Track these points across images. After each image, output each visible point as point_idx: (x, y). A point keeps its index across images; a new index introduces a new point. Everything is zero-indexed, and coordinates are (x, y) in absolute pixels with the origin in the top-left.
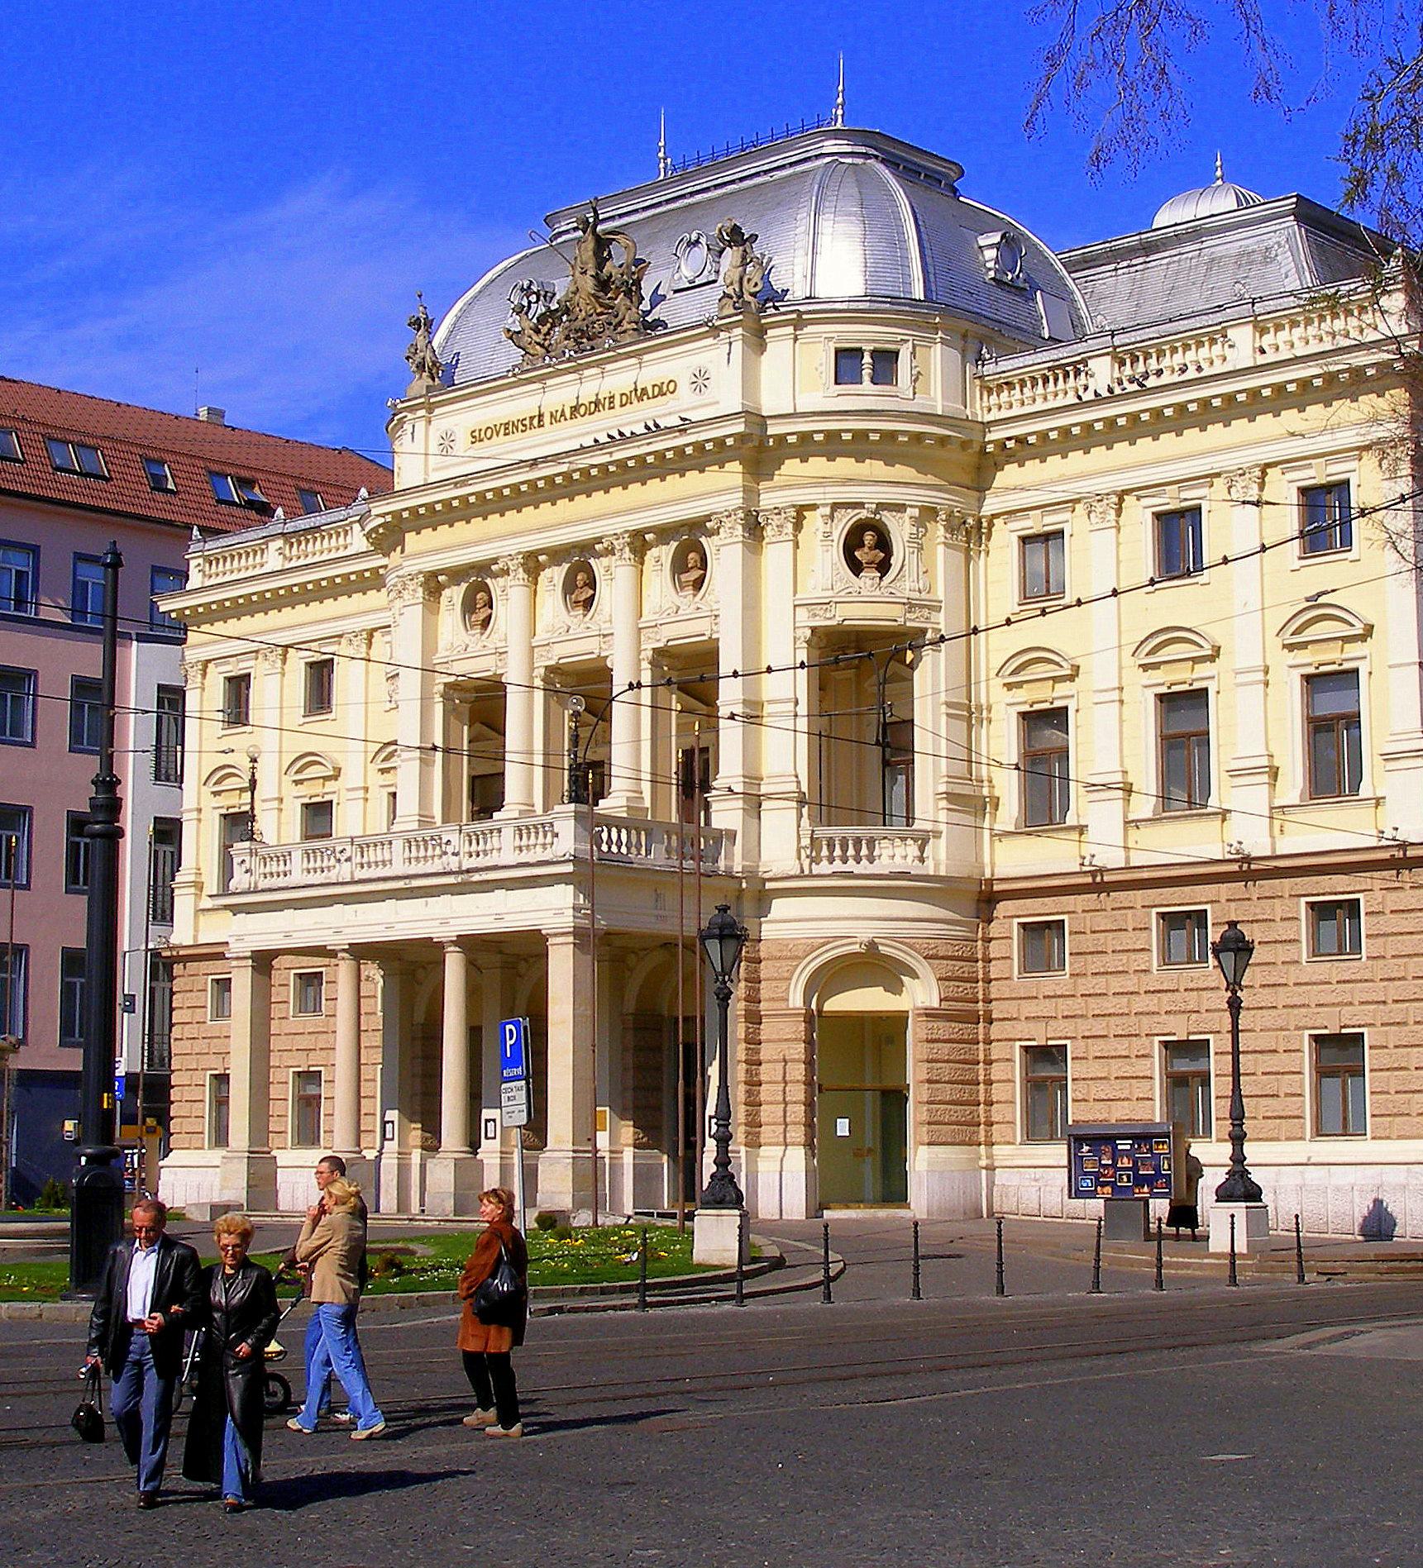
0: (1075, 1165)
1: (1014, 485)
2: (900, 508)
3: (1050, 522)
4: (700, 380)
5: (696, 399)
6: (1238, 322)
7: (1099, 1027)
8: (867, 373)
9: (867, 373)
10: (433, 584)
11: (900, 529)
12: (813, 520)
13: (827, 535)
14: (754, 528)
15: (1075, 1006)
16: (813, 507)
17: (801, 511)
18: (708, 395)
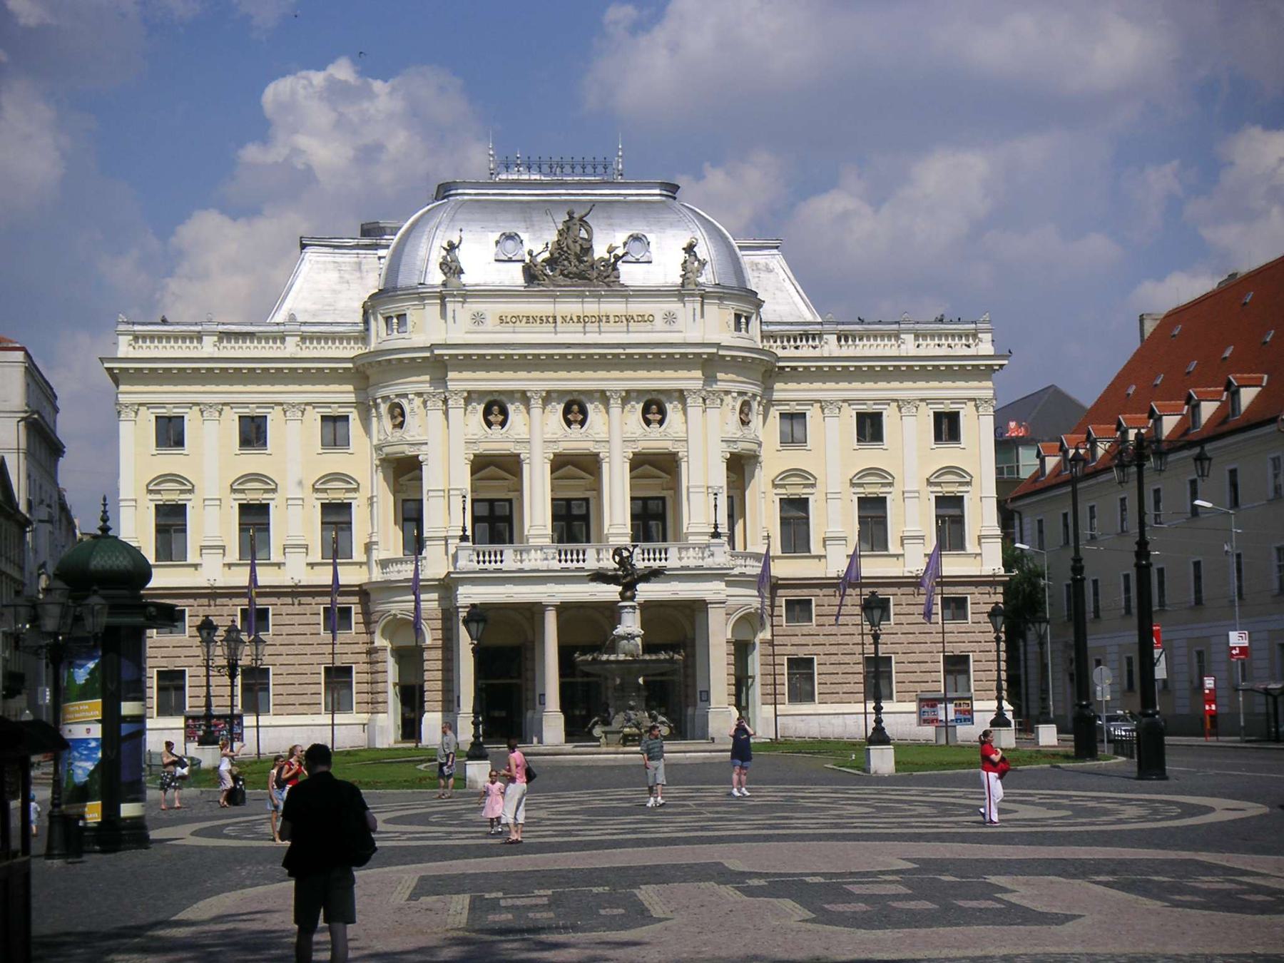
0: (920, 713)
1: (784, 391)
2: (754, 396)
3: (800, 409)
4: (670, 318)
5: (667, 327)
6: (908, 332)
7: (834, 649)
8: (743, 326)
9: (743, 326)
10: (470, 397)
11: (755, 405)
12: (728, 399)
13: (733, 408)
14: (704, 400)
15: (821, 639)
16: (727, 392)
17: (727, 392)
18: (675, 327)
